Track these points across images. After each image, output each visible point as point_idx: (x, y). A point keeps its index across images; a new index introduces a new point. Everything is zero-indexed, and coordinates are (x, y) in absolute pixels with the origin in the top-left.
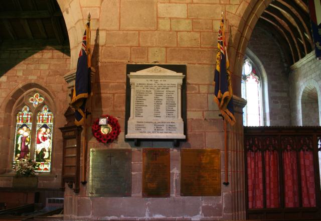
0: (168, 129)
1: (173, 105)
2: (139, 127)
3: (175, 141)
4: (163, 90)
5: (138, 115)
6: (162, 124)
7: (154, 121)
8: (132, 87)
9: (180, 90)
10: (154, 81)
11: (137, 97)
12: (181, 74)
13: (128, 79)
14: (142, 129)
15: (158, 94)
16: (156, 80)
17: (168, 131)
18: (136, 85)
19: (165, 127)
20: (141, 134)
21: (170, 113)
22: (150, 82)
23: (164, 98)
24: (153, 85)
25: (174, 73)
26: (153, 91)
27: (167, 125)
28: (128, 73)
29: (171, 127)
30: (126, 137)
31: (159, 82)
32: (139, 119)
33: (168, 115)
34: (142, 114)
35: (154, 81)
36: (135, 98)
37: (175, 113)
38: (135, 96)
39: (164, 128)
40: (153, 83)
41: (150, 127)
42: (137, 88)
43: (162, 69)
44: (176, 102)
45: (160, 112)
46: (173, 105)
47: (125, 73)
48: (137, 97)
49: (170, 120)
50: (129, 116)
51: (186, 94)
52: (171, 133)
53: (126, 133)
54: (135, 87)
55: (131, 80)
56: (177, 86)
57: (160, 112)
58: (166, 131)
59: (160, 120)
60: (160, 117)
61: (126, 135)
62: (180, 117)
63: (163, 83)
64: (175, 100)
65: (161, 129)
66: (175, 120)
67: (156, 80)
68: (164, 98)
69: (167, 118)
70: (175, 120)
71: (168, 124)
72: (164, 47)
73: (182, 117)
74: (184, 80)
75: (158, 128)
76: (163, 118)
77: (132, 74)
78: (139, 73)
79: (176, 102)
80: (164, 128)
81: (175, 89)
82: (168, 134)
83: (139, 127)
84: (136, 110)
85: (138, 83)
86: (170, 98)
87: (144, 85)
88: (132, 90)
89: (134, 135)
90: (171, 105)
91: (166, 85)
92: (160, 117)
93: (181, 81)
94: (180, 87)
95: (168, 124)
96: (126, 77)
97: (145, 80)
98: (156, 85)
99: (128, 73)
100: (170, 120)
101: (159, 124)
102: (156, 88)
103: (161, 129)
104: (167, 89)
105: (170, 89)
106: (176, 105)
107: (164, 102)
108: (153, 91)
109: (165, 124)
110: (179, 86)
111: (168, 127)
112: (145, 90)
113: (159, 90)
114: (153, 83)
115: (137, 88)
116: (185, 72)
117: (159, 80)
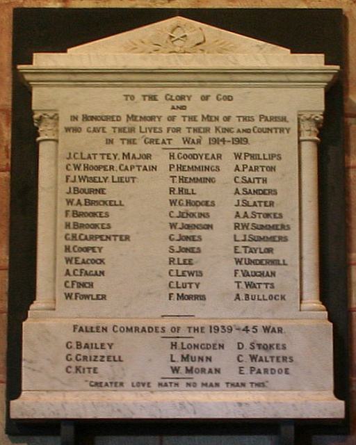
0: (248, 364)
1: (275, 230)
2: (85, 356)
3: (290, 432)
4: (215, 149)
5: (79, 290)
6: (211, 338)
7: (168, 323)
8: (45, 132)
9: (309, 151)
10: (169, 98)
11: (77, 191)
12: (315, 61)
13: (22, 93)
14: (103, 367)
15: (190, 174)
16: (175, 92)
17: (249, 378)
18: (65, 122)
19: (230, 352)
20: (95, 396)
21: (254, 275)
22: (146, 108)
23: (222, 195)
24: (164, 124)
25: (278, 57)
26: (161, 158)
27: (240, 346)
28: (21, 54)
29: (265, 356)
30: (15, 414)
31: (196, 107)
32: (85, 312)
33: (243, 291)
34: (100, 285)
35: (169, 98)
36: (63, 196)
37: (285, 279)
38: (63, 187)
39: (225, 360)
40: (162, 108)
41: (148, 358)
42: (71, 142)
43: (211, 32)
44: (291, 218)
45: (200, 274)
46: (275, 230)
47: (7, 57)
48: (77, 191)
49: (258, 314)
50: (32, 297)
51: (344, 170)
52: (260, 385)
53: (14, 390)
54: (63, 137)
55: (41, 98)
56: (294, 126)
57: (200, 274)
58: (237, 378)
59: (203, 314)
60: (203, 298)
61: (14, 403)
62: (312, 300)
63: (221, 109)
64: (286, 204)
65: (207, 365)
66: (283, 316)
67: (175, 92)
68: (222, 195)
69: (243, 303)
70: (283, 316)
71: (247, 339)
72: (204, 38)
73: (323, 297)
74: (335, 93)
75: (190, 361)
76: (220, 304)
77: (43, 60)
78: (81, 56)
79: (291, 218)
80: (225, 360)
81: (285, 144)
82: (244, 396)
83: (85, 356)
84: (68, 260)
85: (79, 112)
86: (253, 193)
87: (109, 125)
88: (45, 151)
89: (57, 398)
90: (260, 229)
91: (234, 124)
92: (203, 298)
93: (314, 101)
94: (310, 134)
95: (247, 339)
96: (8, 79)
97: (116, 94)
98: (178, 123)
99: (21, 54)
100: (258, 314)
101: (198, 338)
102: (177, 140)
103: (207, 365)
104: (239, 141)
105: (258, 144)
106: (293, 234)
107: (223, 216)
108: (161, 158)
109: (231, 340)
110: (306, 126)
111: (246, 353)
112: (119, 148)
113: (198, 149)
114: (162, 108)
115: (71, 142)
116: (336, 54)
117: (196, 93)
